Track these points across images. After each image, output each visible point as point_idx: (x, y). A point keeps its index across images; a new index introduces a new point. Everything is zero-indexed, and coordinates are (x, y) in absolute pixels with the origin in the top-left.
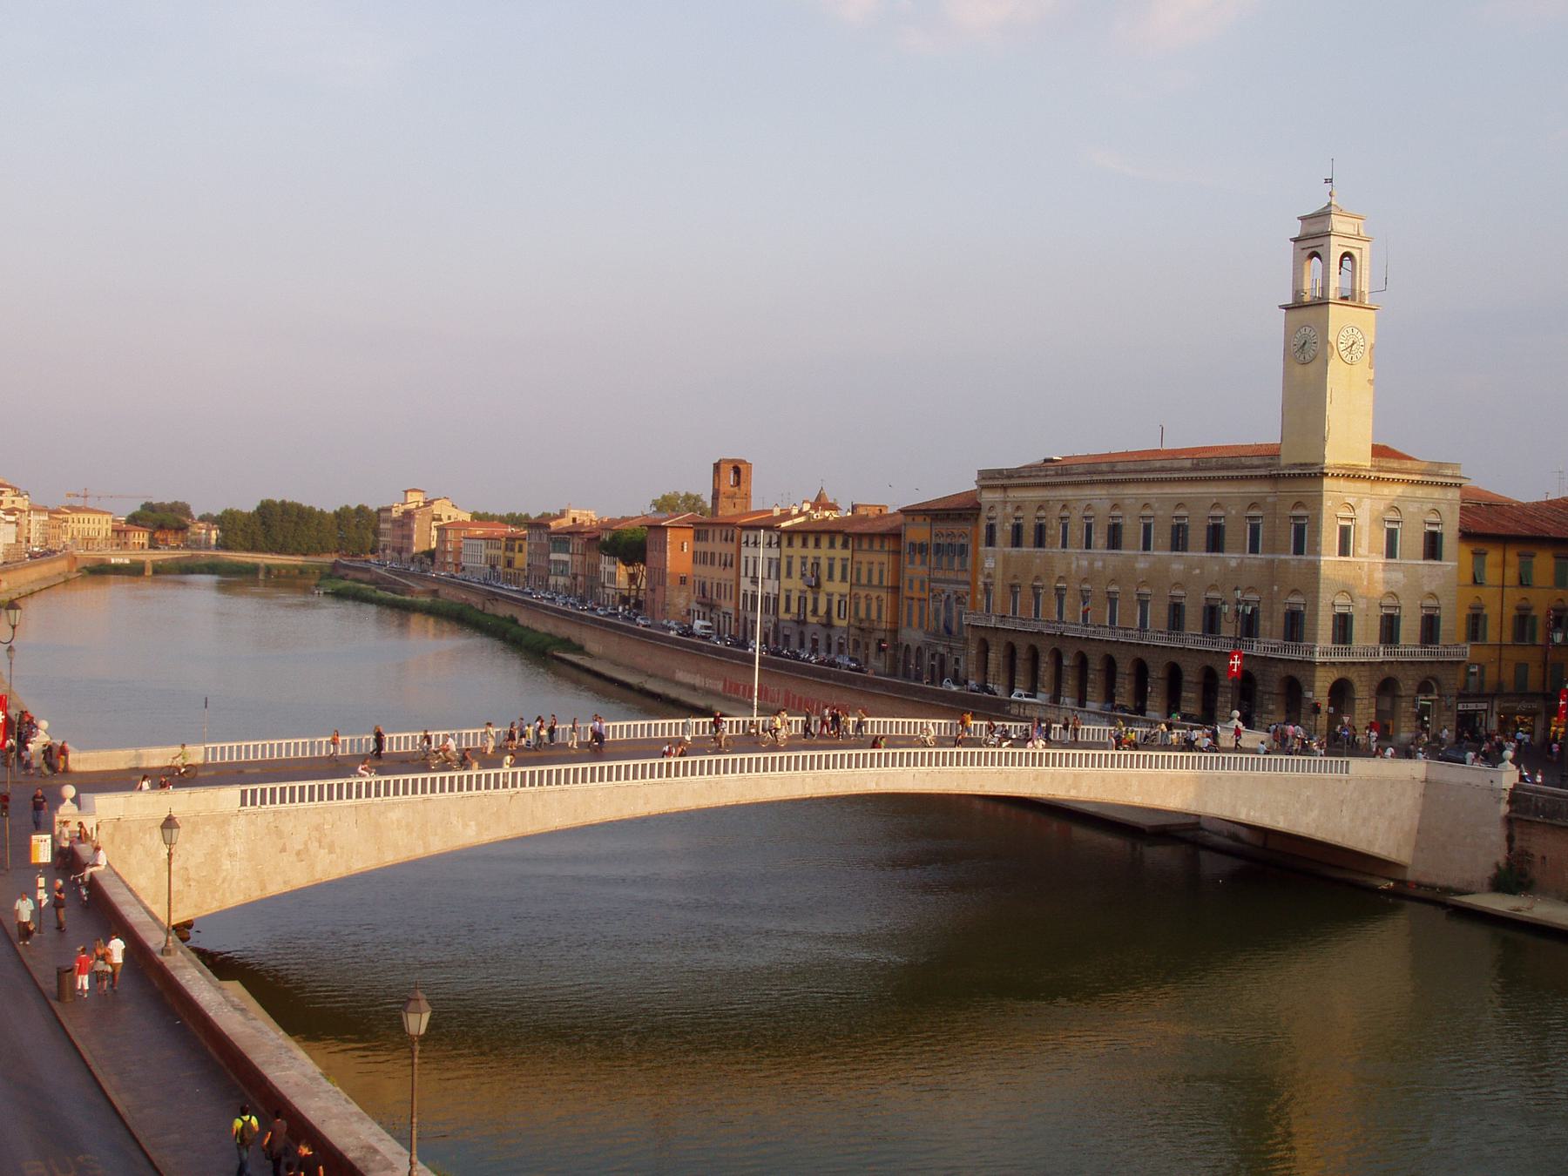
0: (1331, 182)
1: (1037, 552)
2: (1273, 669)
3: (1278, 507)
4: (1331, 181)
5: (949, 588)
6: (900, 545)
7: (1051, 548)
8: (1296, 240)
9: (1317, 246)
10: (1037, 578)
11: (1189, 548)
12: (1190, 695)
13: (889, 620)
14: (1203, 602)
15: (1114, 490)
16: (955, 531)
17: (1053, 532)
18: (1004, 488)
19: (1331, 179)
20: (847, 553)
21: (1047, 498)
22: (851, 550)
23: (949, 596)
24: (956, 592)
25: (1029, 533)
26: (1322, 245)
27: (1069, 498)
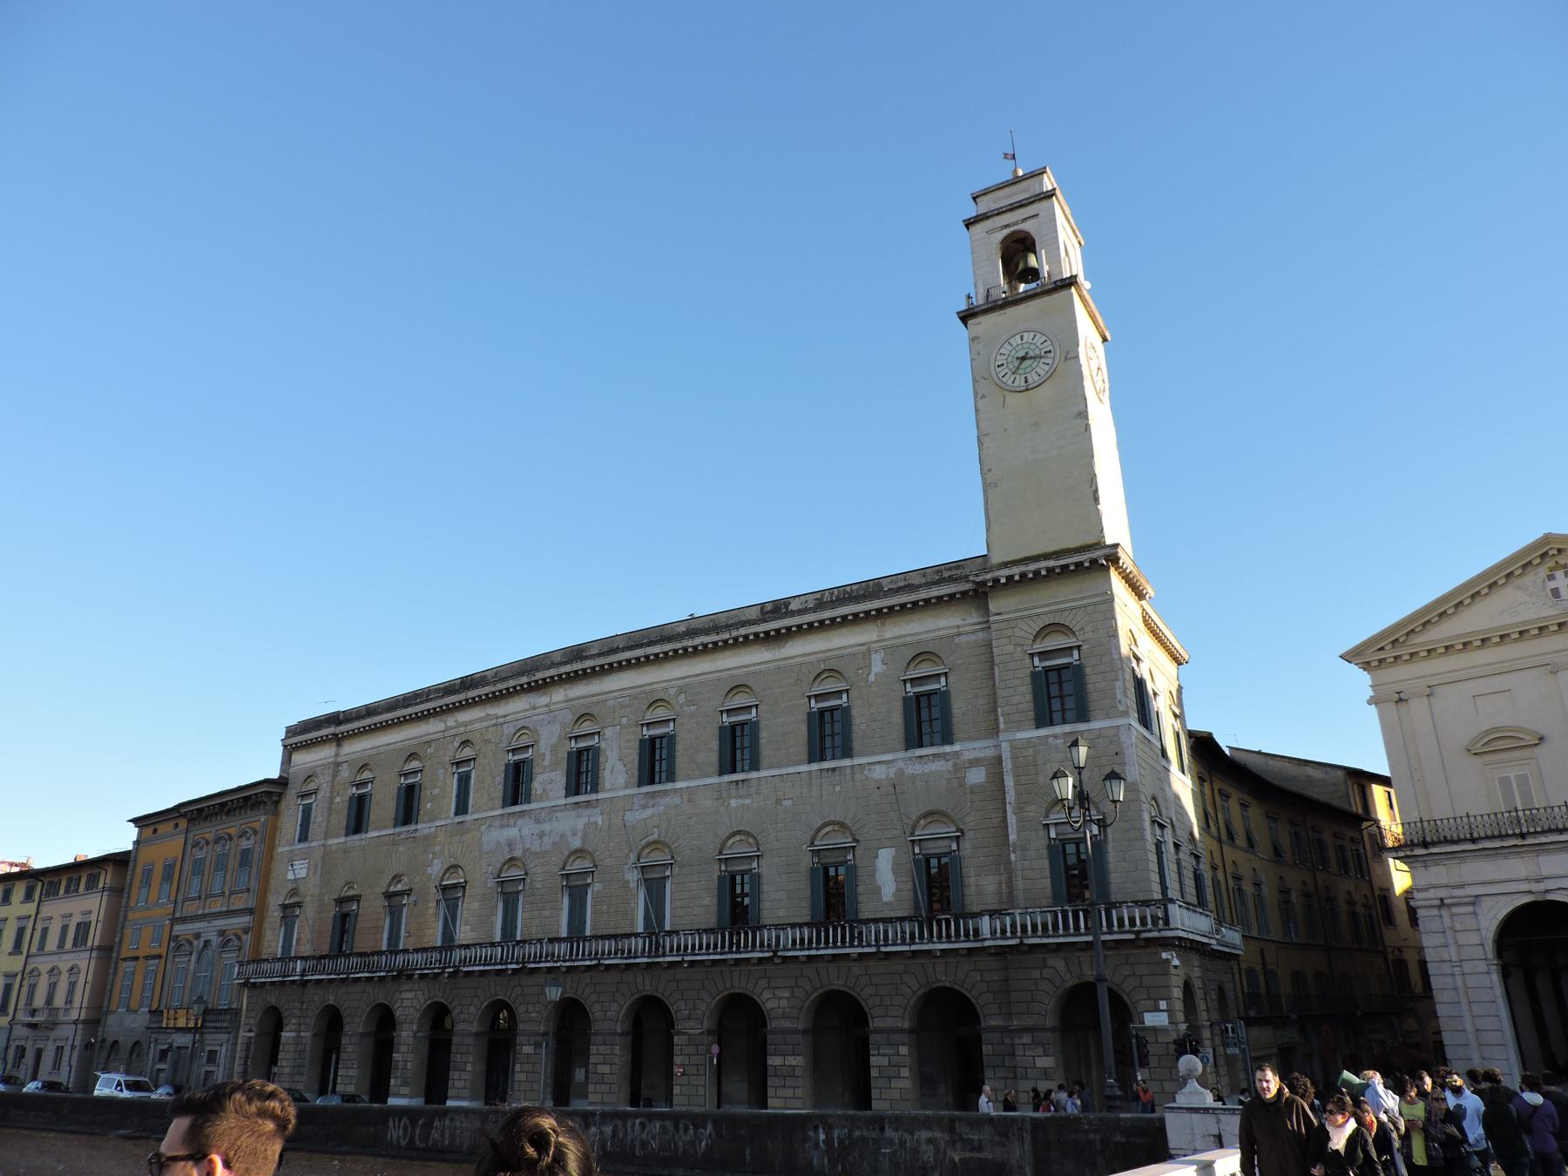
0: (1014, 158)
1: (399, 834)
2: (1036, 974)
3: (994, 643)
4: (1014, 157)
5: (209, 930)
6: (125, 879)
7: (432, 820)
8: (969, 224)
9: (1024, 220)
10: (397, 878)
11: (764, 761)
12: (791, 1061)
13: (85, 1005)
14: (807, 861)
15: (579, 690)
16: (232, 831)
17: (436, 791)
18: (338, 740)
19: (1014, 155)
20: (30, 908)
21: (429, 738)
22: (36, 903)
23: (207, 943)
24: (222, 933)
25: (384, 803)
26: (1037, 215)
27: (477, 726)
